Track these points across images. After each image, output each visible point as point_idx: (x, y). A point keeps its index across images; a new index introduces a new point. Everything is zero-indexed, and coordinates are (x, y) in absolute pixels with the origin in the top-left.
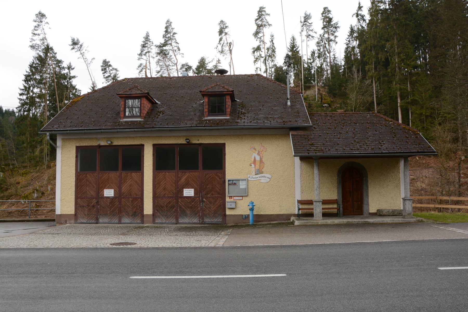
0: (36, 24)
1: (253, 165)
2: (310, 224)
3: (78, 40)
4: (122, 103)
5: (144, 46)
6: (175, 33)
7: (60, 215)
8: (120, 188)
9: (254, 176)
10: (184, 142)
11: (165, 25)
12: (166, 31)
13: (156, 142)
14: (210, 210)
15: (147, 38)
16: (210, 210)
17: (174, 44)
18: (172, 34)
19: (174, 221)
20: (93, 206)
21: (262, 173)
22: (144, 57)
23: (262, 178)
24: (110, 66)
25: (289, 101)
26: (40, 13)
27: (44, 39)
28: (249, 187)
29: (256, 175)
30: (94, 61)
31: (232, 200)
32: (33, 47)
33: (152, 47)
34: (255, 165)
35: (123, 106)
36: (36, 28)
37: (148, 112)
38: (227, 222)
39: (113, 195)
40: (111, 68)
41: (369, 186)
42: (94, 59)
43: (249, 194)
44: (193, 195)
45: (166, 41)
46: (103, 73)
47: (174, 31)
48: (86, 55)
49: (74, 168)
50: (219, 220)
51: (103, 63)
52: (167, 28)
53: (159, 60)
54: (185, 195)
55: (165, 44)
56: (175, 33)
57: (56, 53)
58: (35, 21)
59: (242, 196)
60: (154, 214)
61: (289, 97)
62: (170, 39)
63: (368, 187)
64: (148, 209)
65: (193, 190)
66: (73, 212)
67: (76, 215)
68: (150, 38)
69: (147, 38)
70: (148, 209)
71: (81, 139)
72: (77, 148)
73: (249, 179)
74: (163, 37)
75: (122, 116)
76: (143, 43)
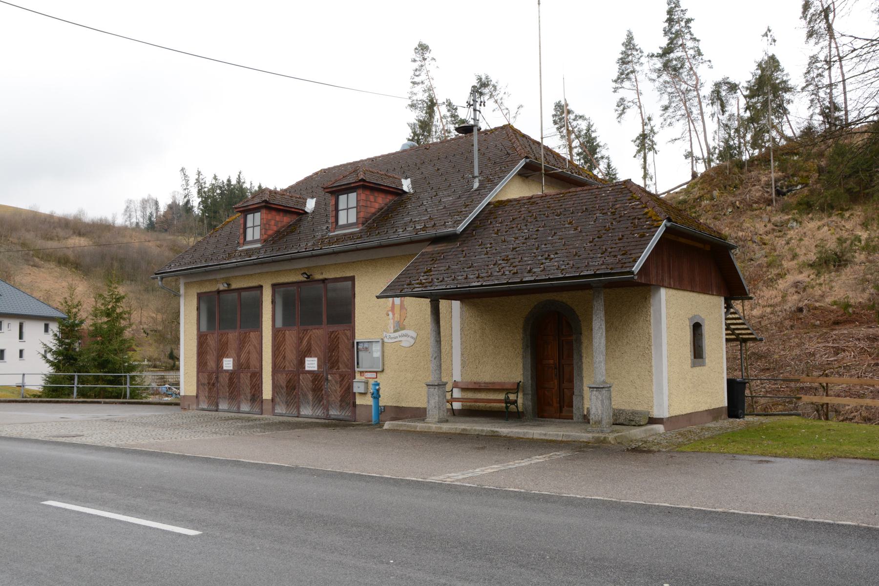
0: (416, 65)
1: (390, 313)
2: (404, 428)
3: (487, 78)
4: (242, 221)
5: (623, 61)
6: (689, 21)
7: (184, 396)
8: (239, 356)
9: (392, 335)
10: (302, 278)
11: (667, 8)
12: (670, 21)
13: (275, 281)
14: (327, 394)
15: (629, 44)
16: (327, 394)
17: (690, 44)
18: (683, 24)
19: (295, 412)
20: (213, 384)
21: (404, 329)
22: (627, 84)
23: (405, 338)
24: (569, 112)
25: (477, 180)
26: (420, 45)
27: (430, 89)
28: (385, 354)
29: (395, 331)
30: (521, 110)
31: (363, 378)
32: (413, 106)
33: (643, 60)
34: (394, 314)
35: (242, 226)
36: (417, 73)
37: (278, 232)
38: (357, 417)
39: (231, 368)
40: (572, 116)
41: (584, 355)
42: (521, 106)
43: (386, 368)
44: (316, 369)
45: (672, 41)
46: (558, 129)
47: (688, 16)
48: (506, 104)
49: (195, 327)
50: (345, 414)
51: (555, 109)
52: (670, 12)
53: (665, 82)
54: (307, 369)
55: (667, 51)
56: (689, 21)
57: (456, 109)
58: (415, 61)
59: (376, 372)
60: (273, 400)
61: (476, 173)
62: (678, 34)
63: (581, 357)
64: (267, 392)
65: (316, 359)
66: (194, 394)
67: (197, 397)
68: (636, 41)
69: (629, 44)
70: (267, 392)
71: (201, 283)
72: (200, 296)
73: (386, 340)
74: (666, 34)
75: (242, 241)
76: (621, 56)
